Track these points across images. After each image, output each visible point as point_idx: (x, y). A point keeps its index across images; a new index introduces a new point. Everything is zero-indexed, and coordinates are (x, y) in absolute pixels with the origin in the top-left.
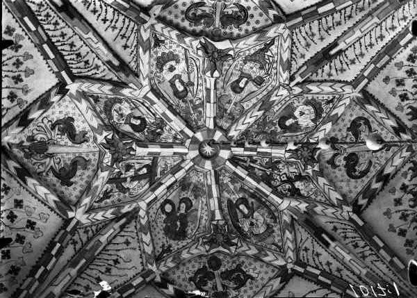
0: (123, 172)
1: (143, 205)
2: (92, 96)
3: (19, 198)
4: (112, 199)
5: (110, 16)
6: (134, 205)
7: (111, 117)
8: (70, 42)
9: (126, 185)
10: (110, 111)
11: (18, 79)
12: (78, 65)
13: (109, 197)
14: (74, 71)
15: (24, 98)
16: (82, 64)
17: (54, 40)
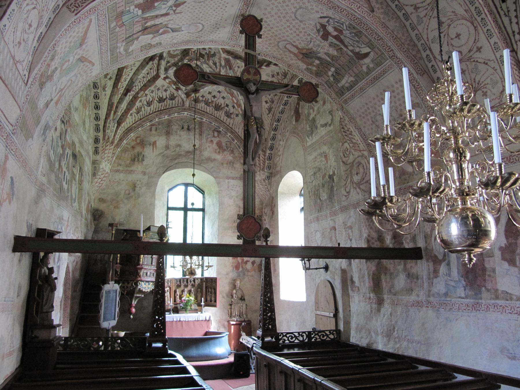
0: (205, 51)
1: (224, 55)
2: (167, 64)
3: (208, 92)
4: (217, 62)
5: (130, 69)
6: (222, 59)
7: (177, 55)
8: (142, 79)
9: (212, 53)
10: (174, 55)
11: (158, 89)
12: (152, 72)
13: (216, 63)
14: (155, 73)
15: (166, 86)
16: (152, 71)
17: (142, 85)
